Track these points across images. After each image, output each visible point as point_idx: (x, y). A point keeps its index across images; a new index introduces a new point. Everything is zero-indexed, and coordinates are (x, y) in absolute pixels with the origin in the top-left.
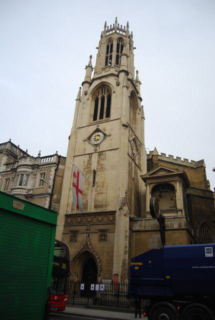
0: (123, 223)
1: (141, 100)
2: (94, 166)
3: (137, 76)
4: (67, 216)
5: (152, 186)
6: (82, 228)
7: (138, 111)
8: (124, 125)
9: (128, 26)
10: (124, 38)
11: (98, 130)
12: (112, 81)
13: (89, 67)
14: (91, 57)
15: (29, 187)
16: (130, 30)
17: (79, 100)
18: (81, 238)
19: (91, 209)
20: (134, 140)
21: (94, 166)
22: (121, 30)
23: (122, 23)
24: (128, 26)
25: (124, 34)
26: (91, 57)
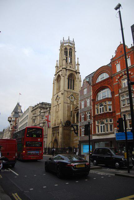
0: (61, 130)
1: (80, 73)
2: (57, 111)
3: (78, 61)
4: (53, 128)
5: (76, 113)
6: (55, 132)
7: (77, 80)
8: (62, 94)
9: (69, 39)
10: (67, 47)
11: (58, 96)
12: (60, 73)
13: (57, 67)
14: (57, 61)
15: (44, 120)
16: (71, 40)
17: (54, 83)
18: (55, 135)
19: (57, 126)
20: (72, 95)
21: (57, 111)
22: (67, 43)
23: (66, 39)
24: (69, 39)
25: (68, 44)
26: (57, 61)
